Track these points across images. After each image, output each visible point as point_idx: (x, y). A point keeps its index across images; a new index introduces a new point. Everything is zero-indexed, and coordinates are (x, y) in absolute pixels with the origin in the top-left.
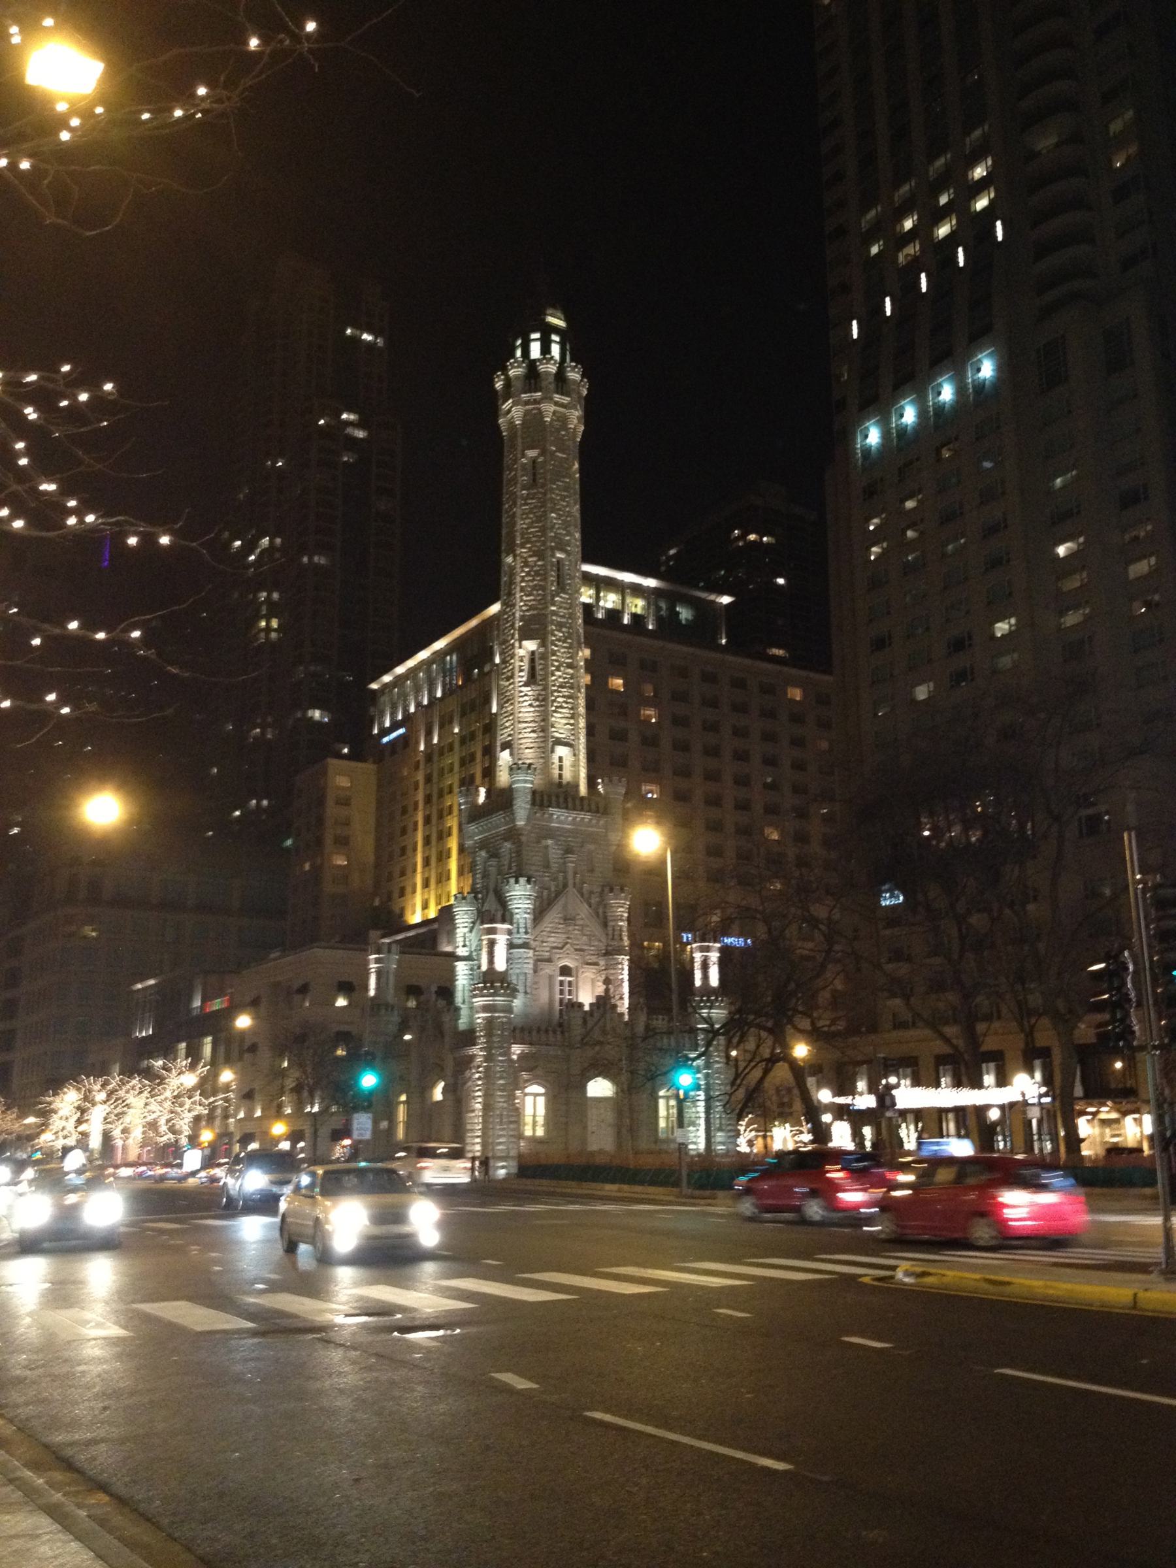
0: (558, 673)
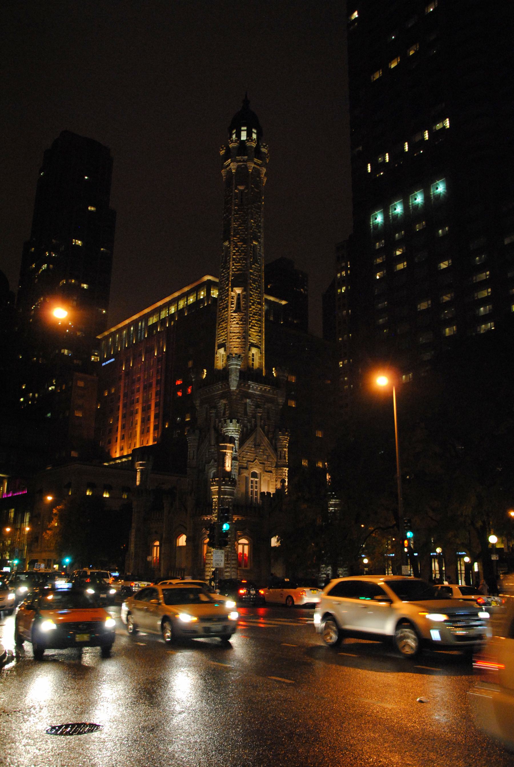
0: (252, 307)
